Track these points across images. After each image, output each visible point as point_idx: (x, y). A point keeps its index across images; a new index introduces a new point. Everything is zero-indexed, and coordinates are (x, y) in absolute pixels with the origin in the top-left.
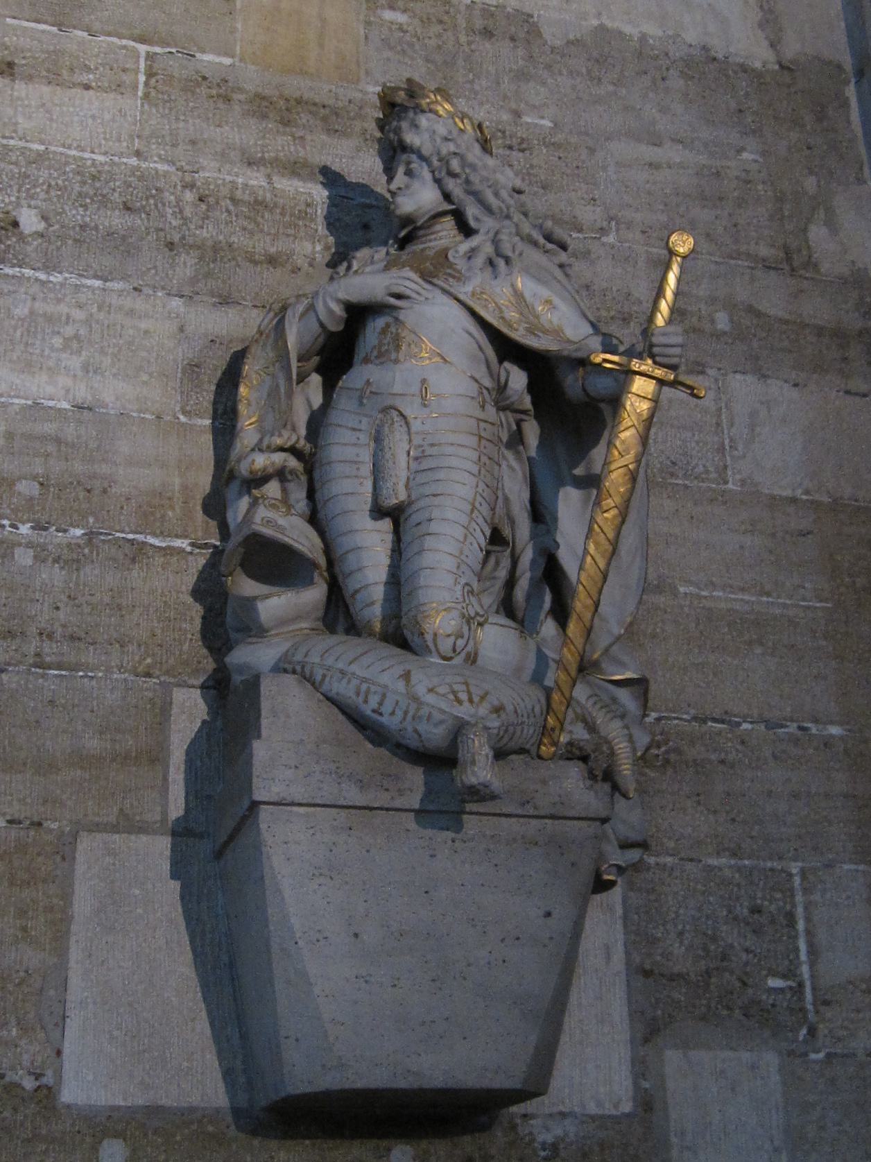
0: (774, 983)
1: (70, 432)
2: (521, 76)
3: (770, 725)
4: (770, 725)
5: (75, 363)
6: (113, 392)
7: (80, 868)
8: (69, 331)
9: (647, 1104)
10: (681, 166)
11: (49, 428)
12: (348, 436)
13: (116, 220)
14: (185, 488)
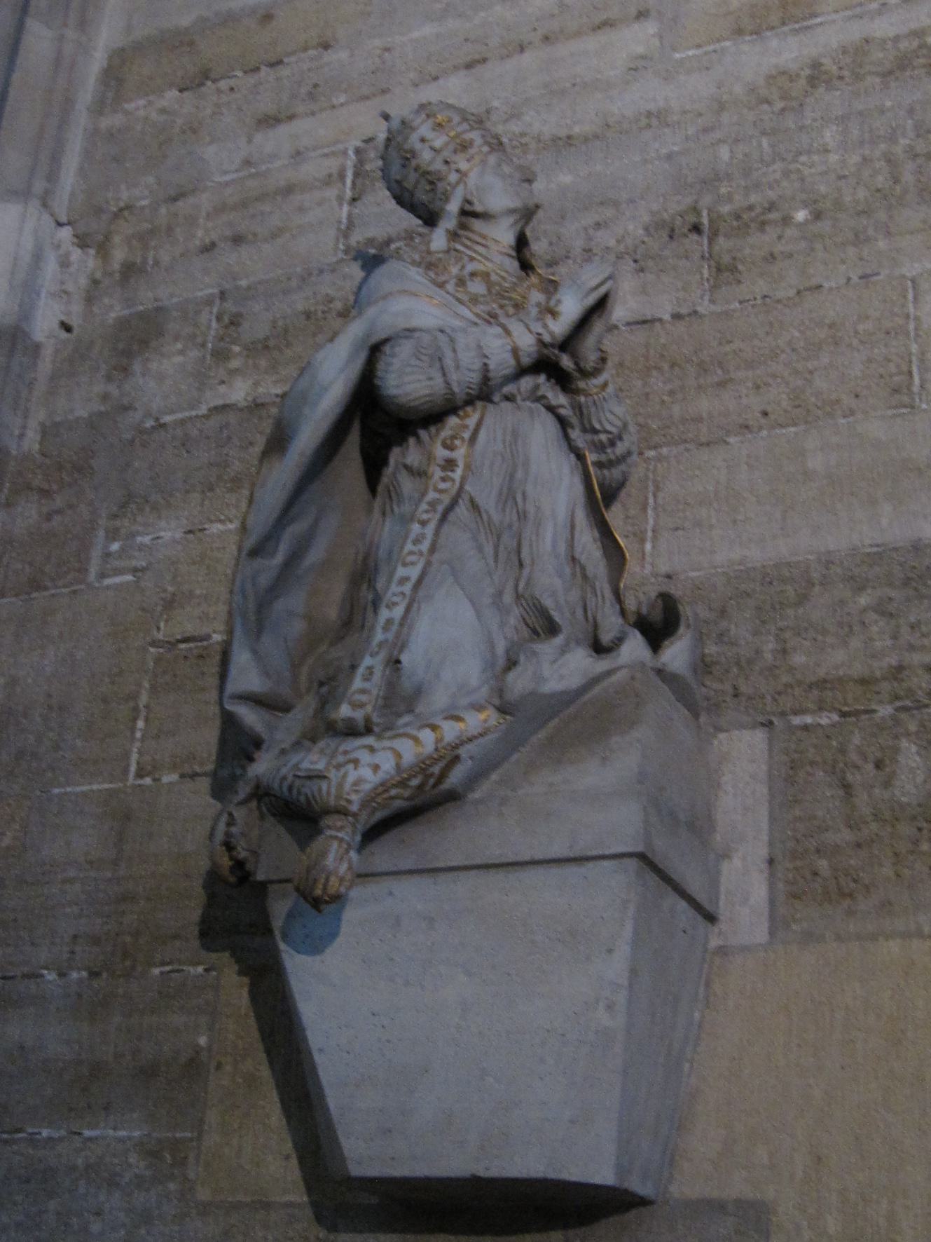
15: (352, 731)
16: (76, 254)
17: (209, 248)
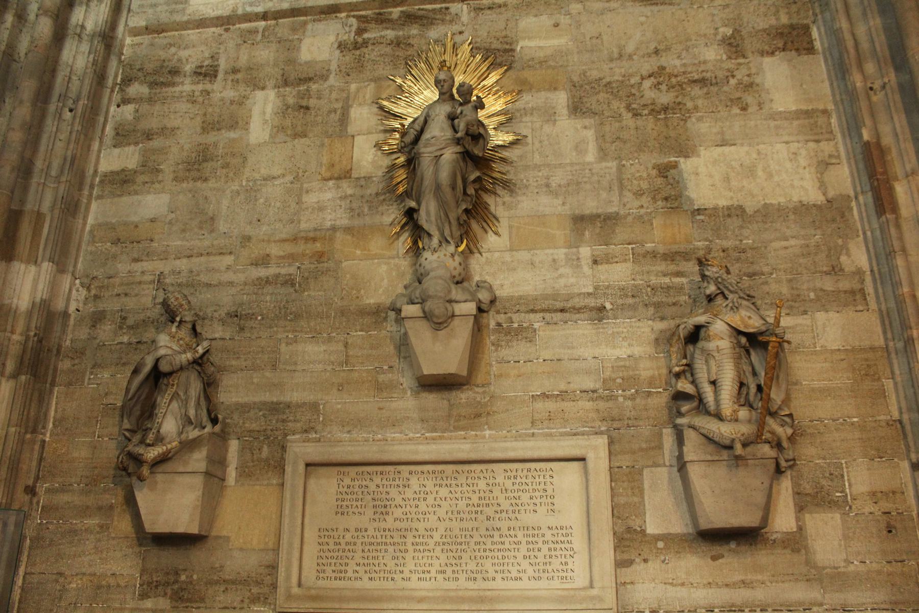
0: (838, 494)
1: (627, 364)
2: (741, 227)
3: (834, 420)
4: (834, 420)
5: (626, 344)
6: (637, 350)
7: (645, 477)
8: (623, 335)
9: (800, 528)
10: (795, 246)
11: (622, 363)
12: (700, 362)
13: (630, 301)
14: (659, 375)
15: (149, 445)
16: (81, 289)
17: (119, 295)
